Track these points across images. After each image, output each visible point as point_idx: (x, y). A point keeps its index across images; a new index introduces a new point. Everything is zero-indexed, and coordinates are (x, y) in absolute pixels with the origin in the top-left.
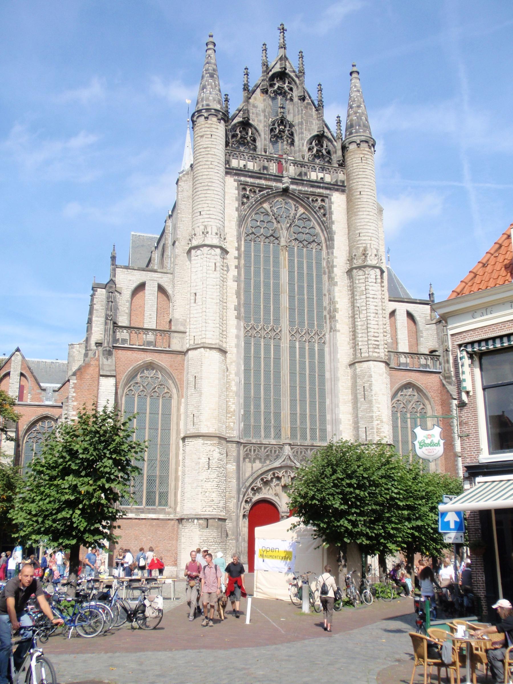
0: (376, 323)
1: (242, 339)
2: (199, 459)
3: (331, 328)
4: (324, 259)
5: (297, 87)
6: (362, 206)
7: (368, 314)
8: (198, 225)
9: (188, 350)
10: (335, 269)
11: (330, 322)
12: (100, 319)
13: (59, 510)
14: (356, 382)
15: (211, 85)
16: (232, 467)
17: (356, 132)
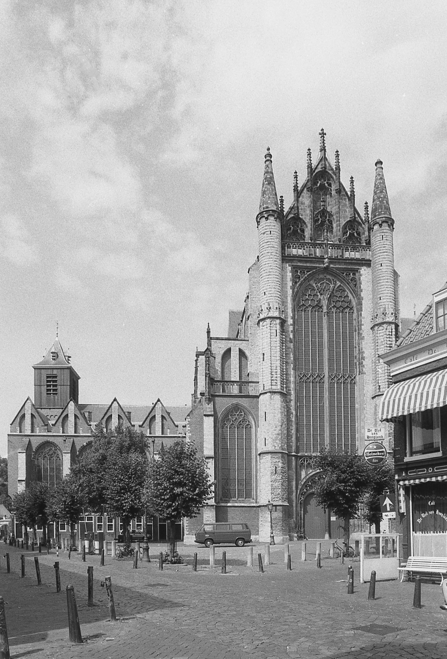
5: (335, 182)
9: (261, 394)
10: (363, 327)
17: (379, 215)
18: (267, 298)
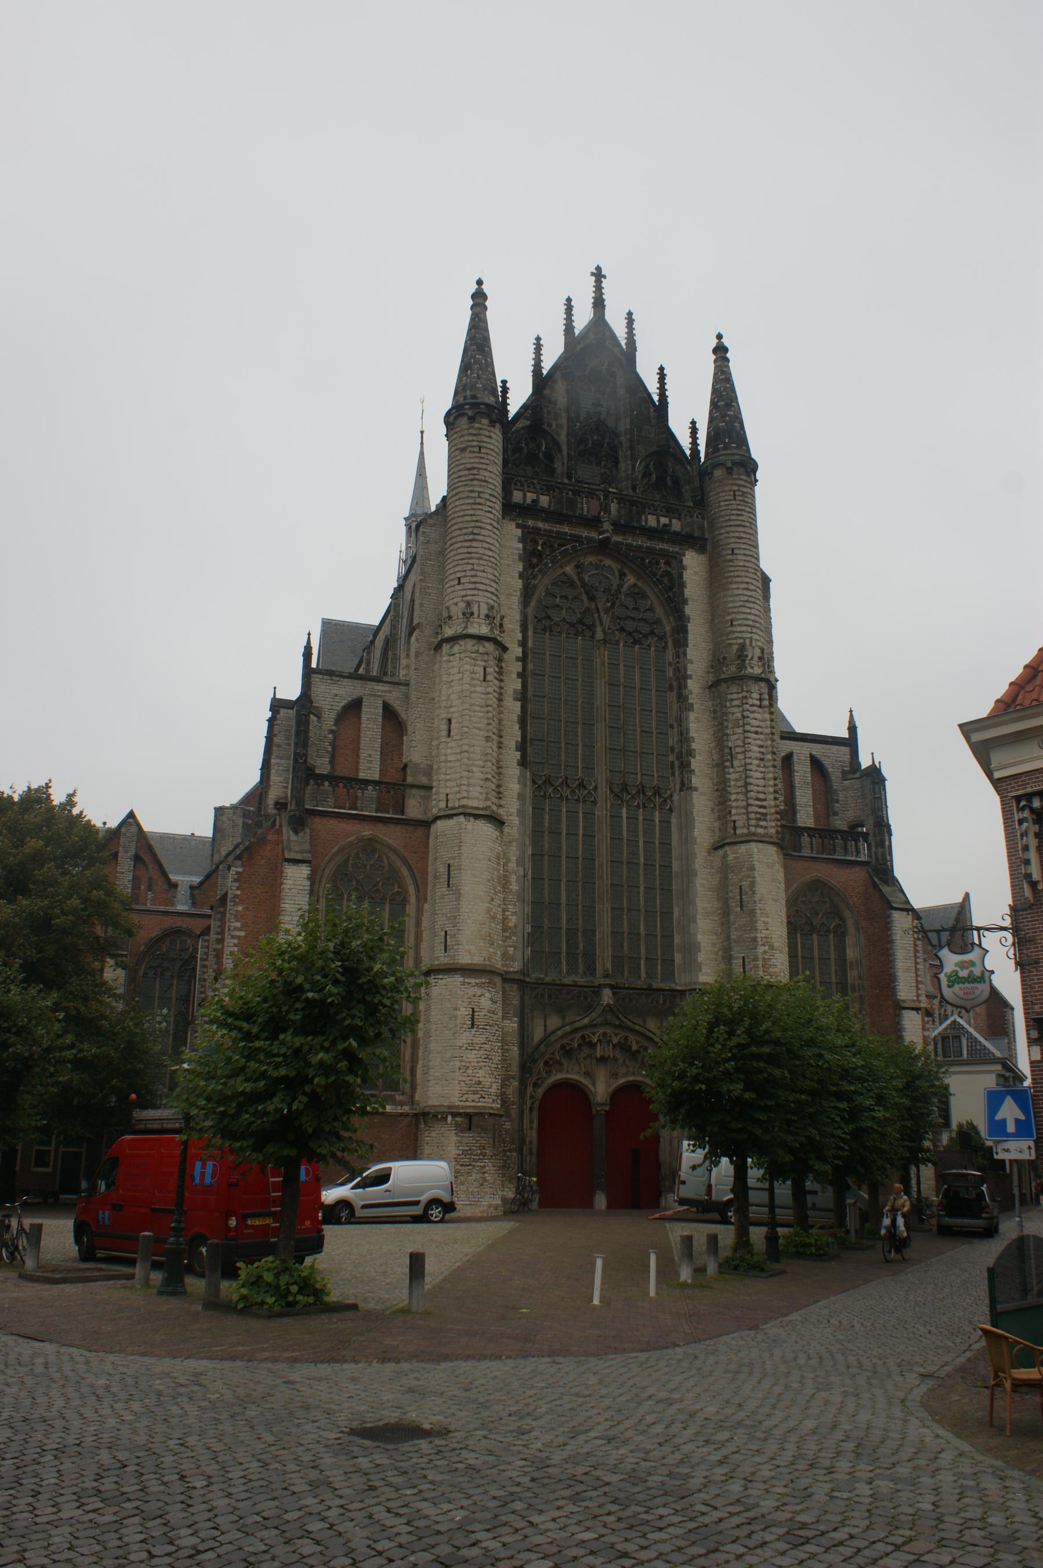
0: (762, 775)
1: (528, 801)
2: (456, 1009)
3: (683, 784)
4: (670, 664)
6: (736, 574)
7: (748, 761)
8: (455, 600)
10: (689, 682)
11: (682, 773)
12: (283, 761)
13: (266, 1096)
14: (727, 878)
15: (480, 363)
16: (512, 1025)
17: (725, 448)
18: (464, 593)
